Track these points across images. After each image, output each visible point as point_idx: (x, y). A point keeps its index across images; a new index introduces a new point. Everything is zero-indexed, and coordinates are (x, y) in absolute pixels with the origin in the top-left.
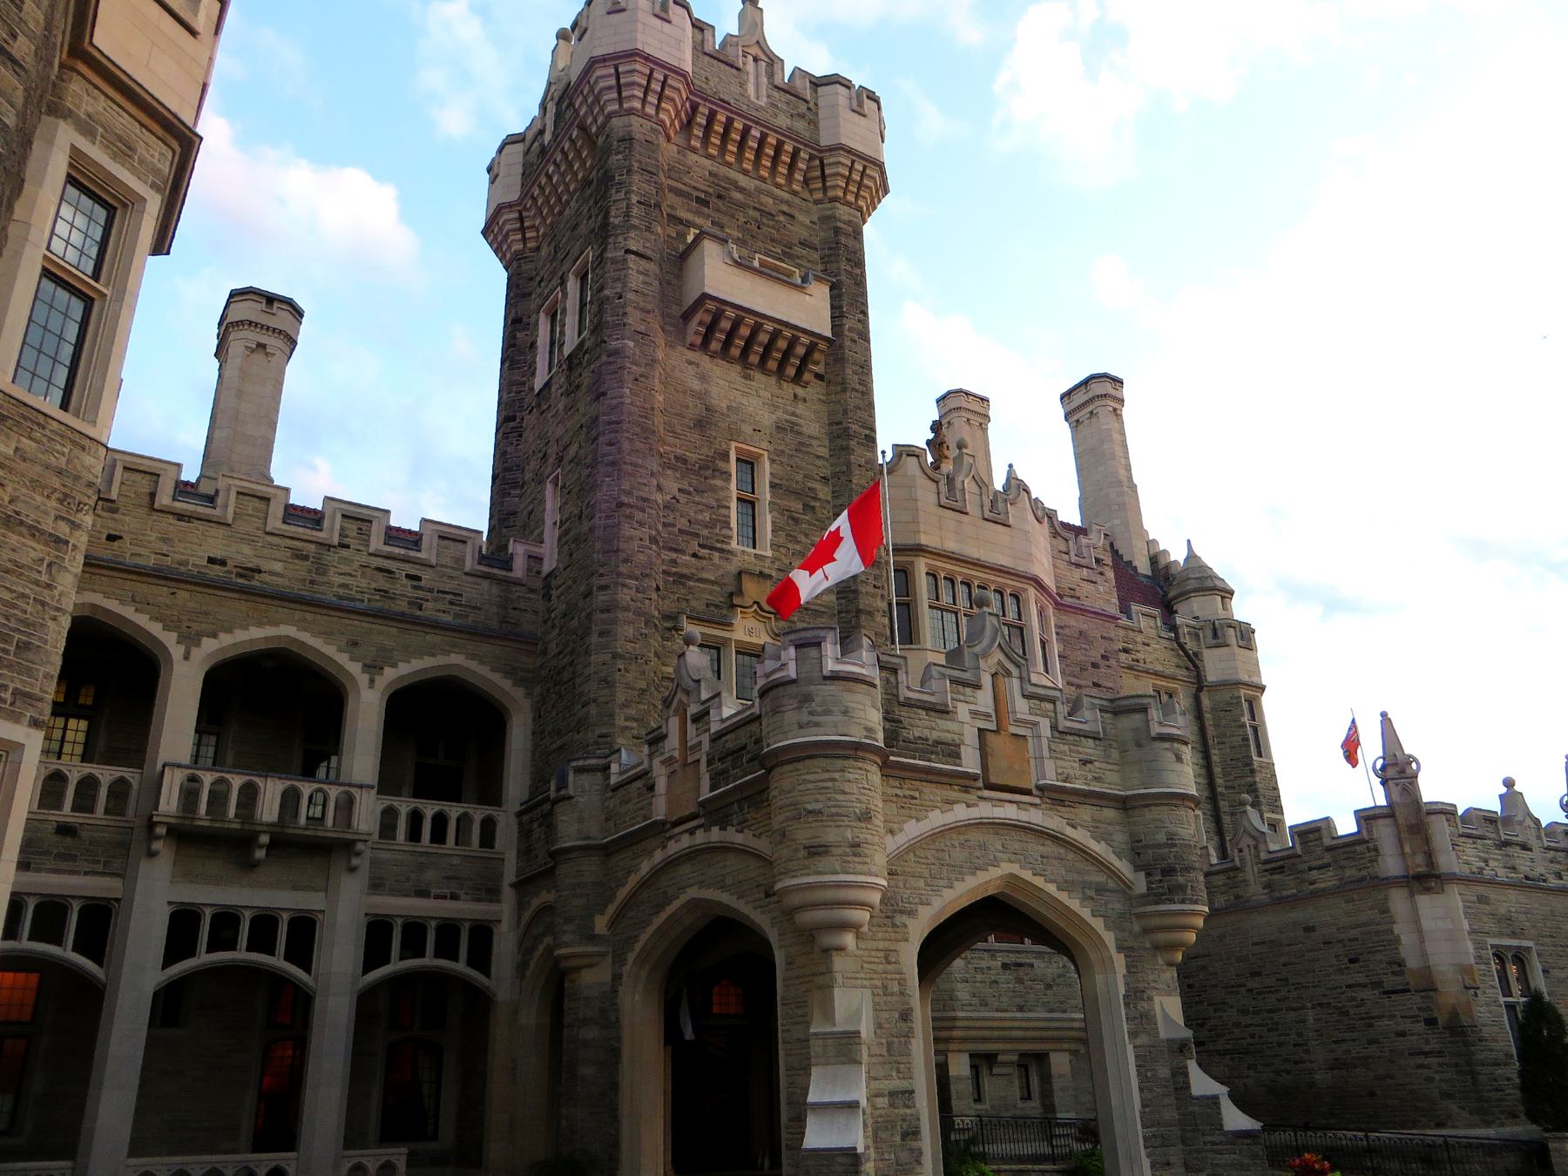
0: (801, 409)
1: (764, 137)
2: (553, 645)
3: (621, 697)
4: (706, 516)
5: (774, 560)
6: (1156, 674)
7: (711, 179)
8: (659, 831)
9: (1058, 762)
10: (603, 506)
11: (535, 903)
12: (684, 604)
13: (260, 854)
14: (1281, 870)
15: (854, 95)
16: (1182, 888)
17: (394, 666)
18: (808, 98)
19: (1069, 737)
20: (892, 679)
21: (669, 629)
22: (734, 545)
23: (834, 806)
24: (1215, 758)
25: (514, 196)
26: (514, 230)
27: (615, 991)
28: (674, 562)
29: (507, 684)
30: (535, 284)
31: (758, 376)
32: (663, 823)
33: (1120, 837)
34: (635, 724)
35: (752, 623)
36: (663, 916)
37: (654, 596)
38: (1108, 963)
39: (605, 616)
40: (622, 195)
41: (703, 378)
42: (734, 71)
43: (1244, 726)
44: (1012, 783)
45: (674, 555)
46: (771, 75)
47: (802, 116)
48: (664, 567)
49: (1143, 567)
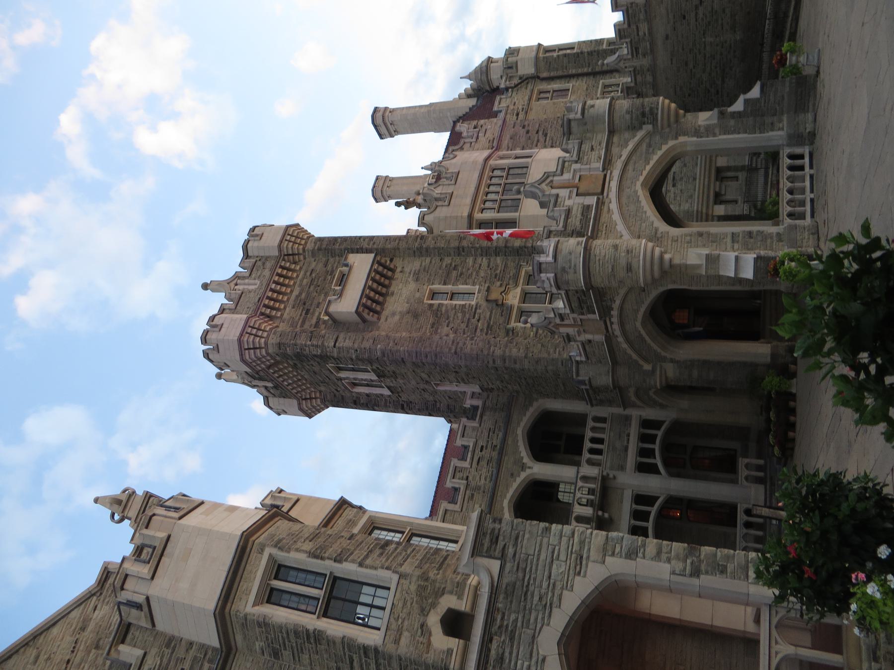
0: (407, 270)
1: (275, 282)
2: (515, 387)
3: (545, 355)
4: (460, 315)
5: (480, 285)
6: (530, 99)
7: (296, 307)
8: (609, 339)
9: (592, 160)
10: (456, 360)
11: (633, 398)
12: (501, 326)
13: (606, 515)
14: (637, 49)
15: (253, 238)
16: (651, 109)
17: (522, 458)
18: (254, 260)
19: (581, 155)
20: (554, 233)
21: (513, 333)
22: (473, 303)
23: (611, 260)
24: (574, 72)
25: (295, 402)
26: (311, 402)
27: (678, 362)
28: (482, 330)
29: (531, 410)
30: (337, 393)
31: (392, 289)
32: (606, 336)
33: (627, 135)
34: (558, 349)
35: (510, 296)
36: (647, 338)
37: (498, 339)
38: (684, 144)
39: (507, 362)
40: (307, 349)
41: (394, 314)
42: (243, 295)
43: (558, 56)
44: (601, 182)
45: (478, 330)
46: (244, 278)
47: (264, 264)
48: (484, 335)
49: (473, 102)
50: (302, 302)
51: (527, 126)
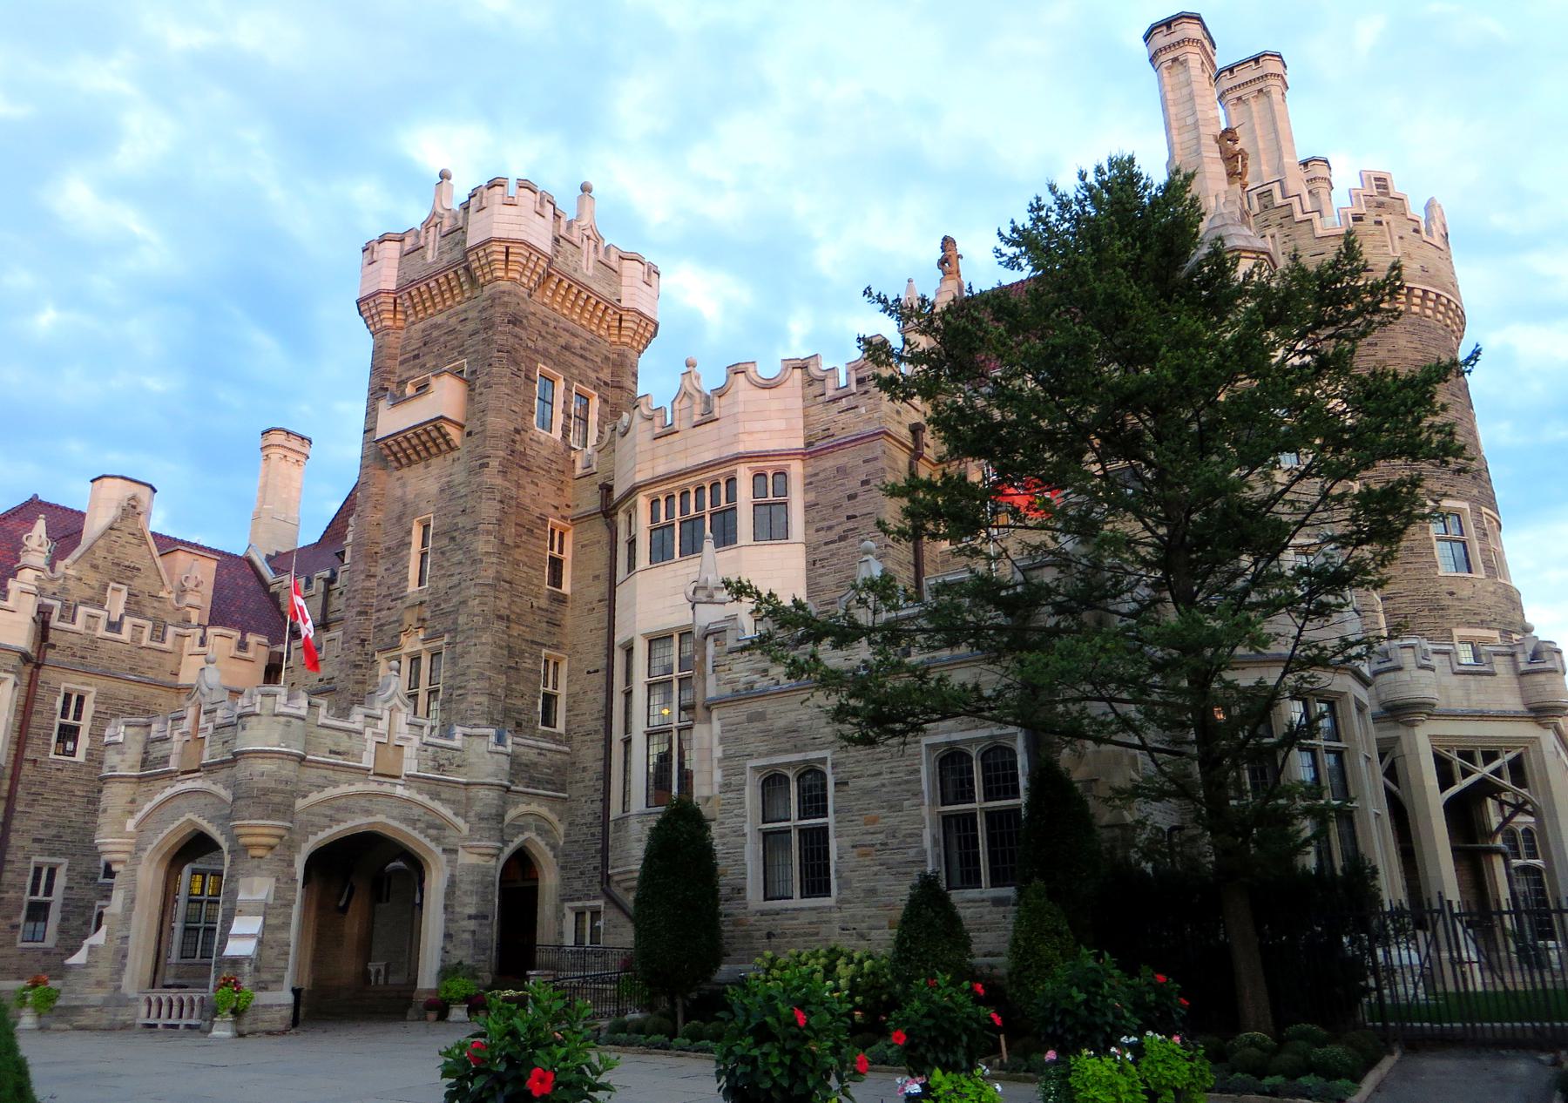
0: (457, 467)
4: (397, 580)
22: (409, 590)
31: (433, 461)
35: (413, 638)
50: (427, 339)
51: (867, 487)
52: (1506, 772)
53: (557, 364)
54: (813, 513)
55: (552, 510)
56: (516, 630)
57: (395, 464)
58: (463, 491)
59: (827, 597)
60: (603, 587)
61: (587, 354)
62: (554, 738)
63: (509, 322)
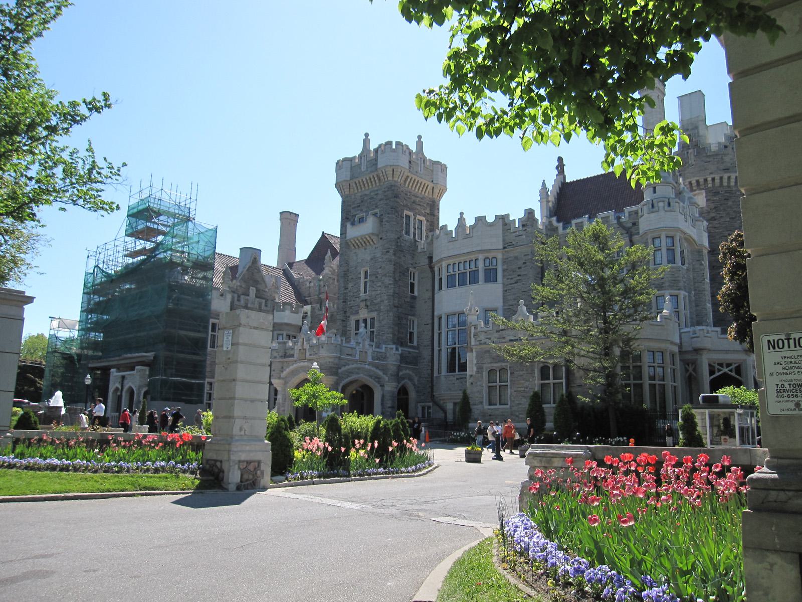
4: (355, 291)
22: (361, 295)
52: (734, 371)
53: (411, 209)
54: (506, 273)
55: (411, 265)
56: (400, 310)
57: (353, 248)
58: (380, 260)
59: (511, 303)
60: (430, 294)
61: (421, 204)
62: (413, 347)
63: (395, 197)
